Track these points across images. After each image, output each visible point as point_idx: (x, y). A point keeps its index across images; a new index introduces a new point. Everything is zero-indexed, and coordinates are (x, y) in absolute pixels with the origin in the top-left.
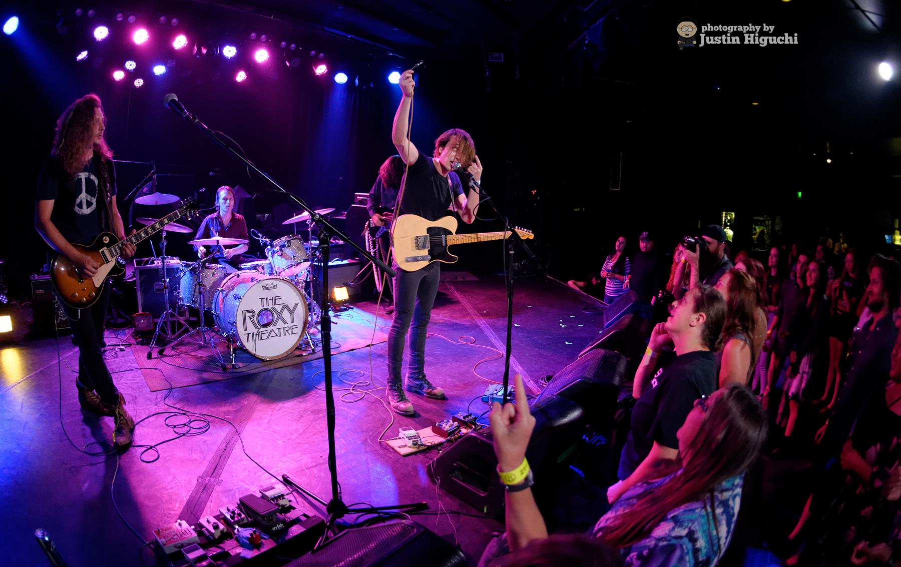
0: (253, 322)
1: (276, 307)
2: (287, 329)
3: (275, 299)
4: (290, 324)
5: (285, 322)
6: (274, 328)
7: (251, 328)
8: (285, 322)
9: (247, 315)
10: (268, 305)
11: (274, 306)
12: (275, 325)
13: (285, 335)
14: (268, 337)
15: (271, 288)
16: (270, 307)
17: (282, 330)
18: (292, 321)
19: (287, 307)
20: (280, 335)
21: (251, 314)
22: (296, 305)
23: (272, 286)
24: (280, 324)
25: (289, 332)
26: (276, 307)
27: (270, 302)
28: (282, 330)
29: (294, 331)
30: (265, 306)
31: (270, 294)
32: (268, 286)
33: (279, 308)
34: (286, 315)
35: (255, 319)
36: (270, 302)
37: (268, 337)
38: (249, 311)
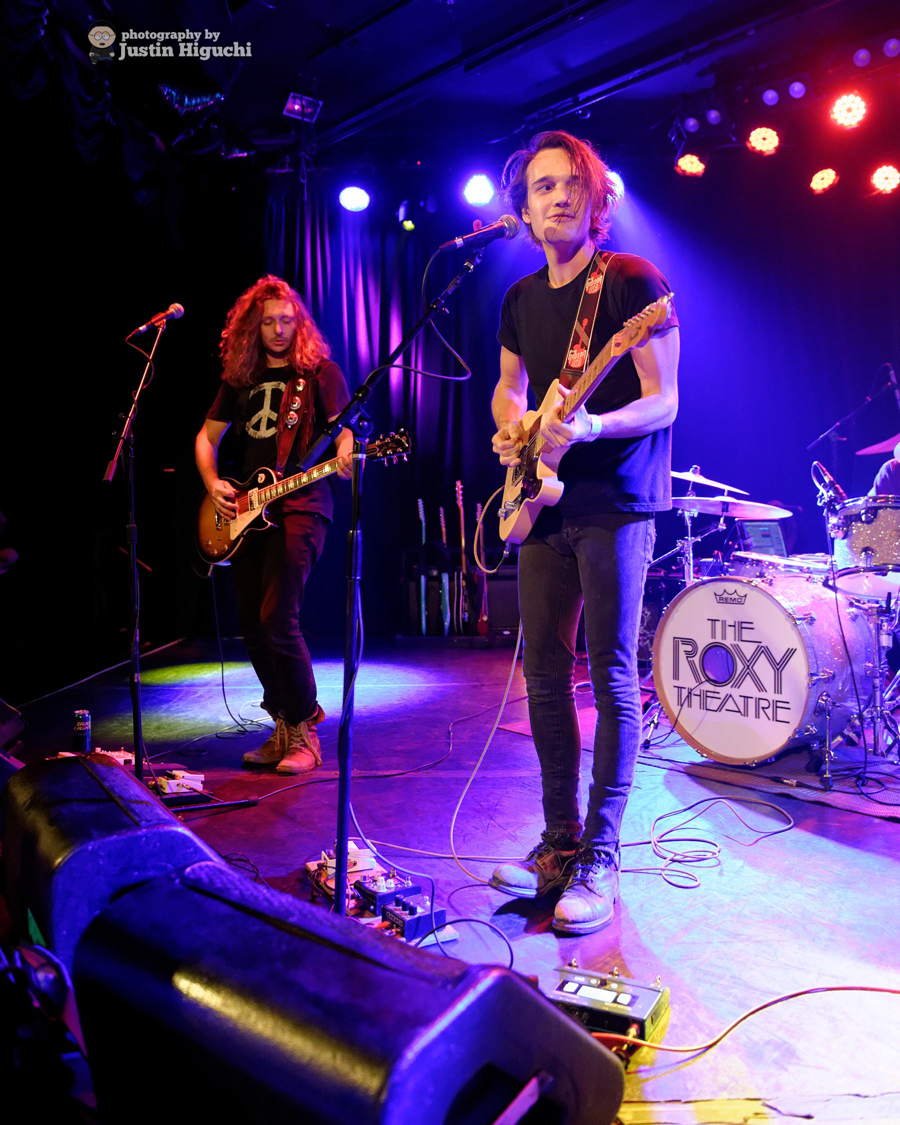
0: (692, 665)
1: (741, 644)
2: (764, 704)
3: (741, 626)
4: (771, 695)
5: (760, 687)
6: (735, 692)
7: (687, 679)
8: (760, 687)
9: (683, 648)
10: (724, 636)
11: (736, 642)
12: (738, 685)
13: (757, 716)
14: (719, 709)
15: (734, 601)
16: (729, 641)
17: (752, 703)
18: (778, 689)
19: (763, 650)
20: (746, 714)
21: (689, 648)
22: (790, 653)
23: (735, 596)
24: (748, 689)
25: (769, 712)
26: (741, 644)
27: (730, 631)
28: (752, 703)
29: (782, 714)
30: (719, 639)
31: (729, 613)
32: (725, 596)
33: (748, 650)
34: (763, 668)
35: (696, 659)
36: (730, 631)
37: (719, 709)
38: (687, 641)
